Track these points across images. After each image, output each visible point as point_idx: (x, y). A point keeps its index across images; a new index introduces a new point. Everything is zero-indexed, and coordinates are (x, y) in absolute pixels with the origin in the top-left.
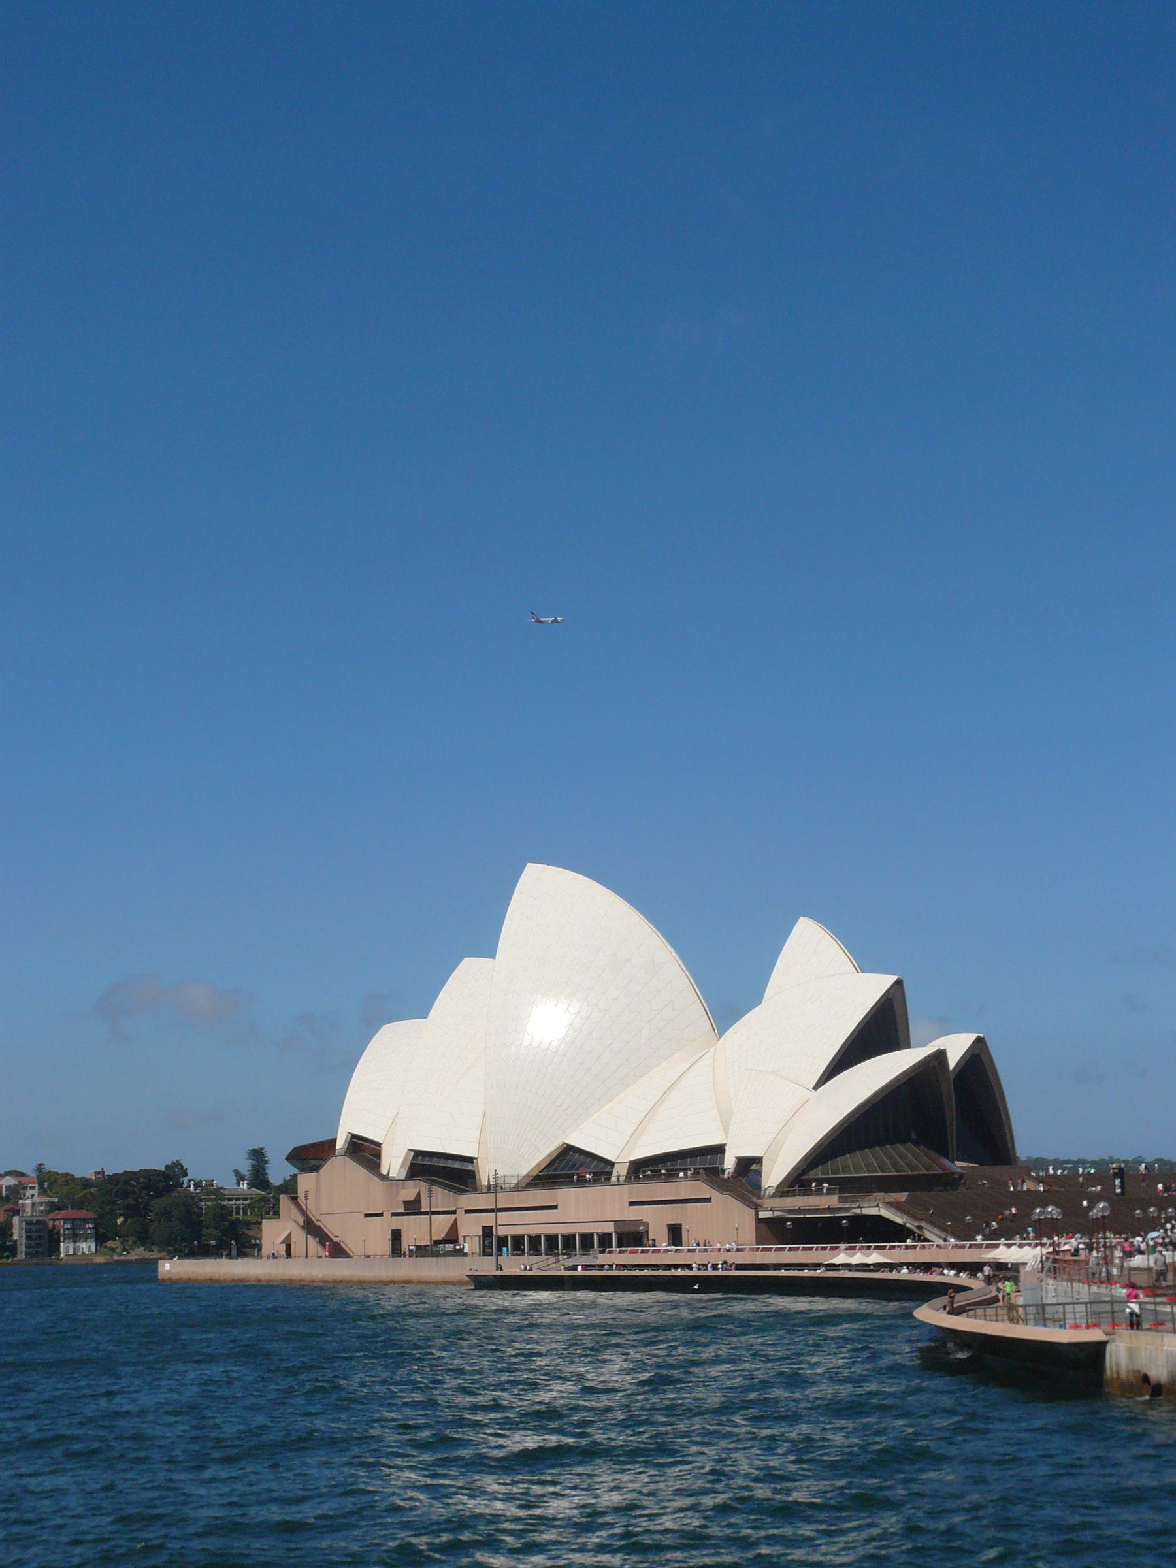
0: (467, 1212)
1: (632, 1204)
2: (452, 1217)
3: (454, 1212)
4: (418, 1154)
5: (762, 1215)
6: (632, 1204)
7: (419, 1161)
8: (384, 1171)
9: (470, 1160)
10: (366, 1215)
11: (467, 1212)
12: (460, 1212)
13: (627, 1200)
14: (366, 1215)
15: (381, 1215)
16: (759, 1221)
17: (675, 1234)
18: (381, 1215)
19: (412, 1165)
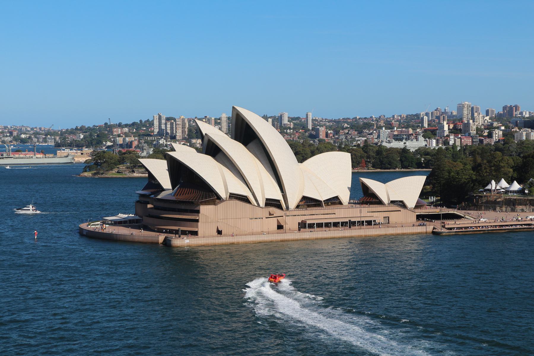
4: (267, 200)
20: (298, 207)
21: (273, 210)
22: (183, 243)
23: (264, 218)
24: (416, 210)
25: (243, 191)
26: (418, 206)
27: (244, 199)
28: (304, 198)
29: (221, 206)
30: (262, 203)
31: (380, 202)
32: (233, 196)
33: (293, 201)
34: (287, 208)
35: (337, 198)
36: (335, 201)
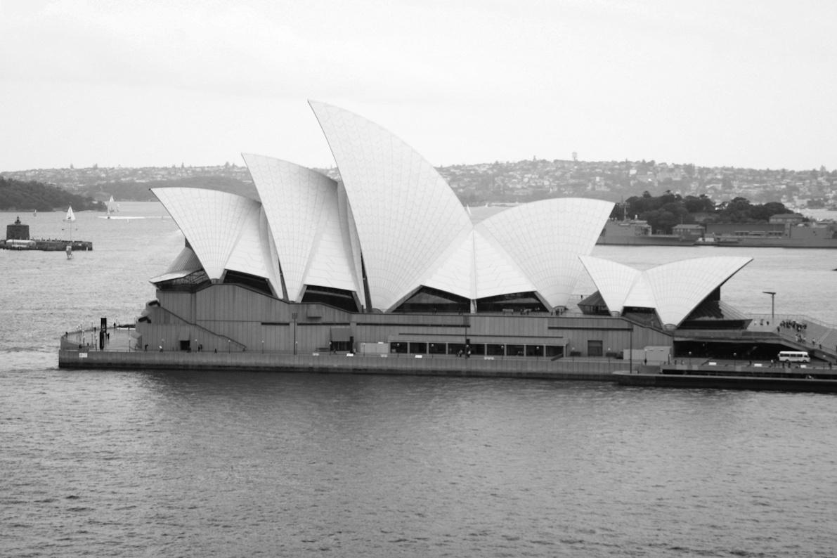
0: (358, 324)
1: (550, 328)
2: (348, 327)
3: (349, 324)
4: (309, 287)
5: (677, 339)
6: (550, 328)
7: (308, 291)
8: (281, 296)
9: (349, 293)
10: (263, 324)
11: (358, 324)
12: (353, 325)
13: (546, 325)
14: (263, 324)
15: (288, 324)
16: (675, 342)
17: (595, 349)
18: (288, 324)
19: (306, 294)
20: (402, 308)
21: (314, 309)
22: (75, 357)
23: (292, 325)
24: (678, 333)
25: (255, 267)
26: (687, 323)
27: (259, 285)
28: (424, 290)
29: (202, 295)
30: (295, 294)
31: (606, 312)
32: (232, 277)
33: (388, 292)
34: (370, 309)
35: (531, 294)
36: (528, 303)
